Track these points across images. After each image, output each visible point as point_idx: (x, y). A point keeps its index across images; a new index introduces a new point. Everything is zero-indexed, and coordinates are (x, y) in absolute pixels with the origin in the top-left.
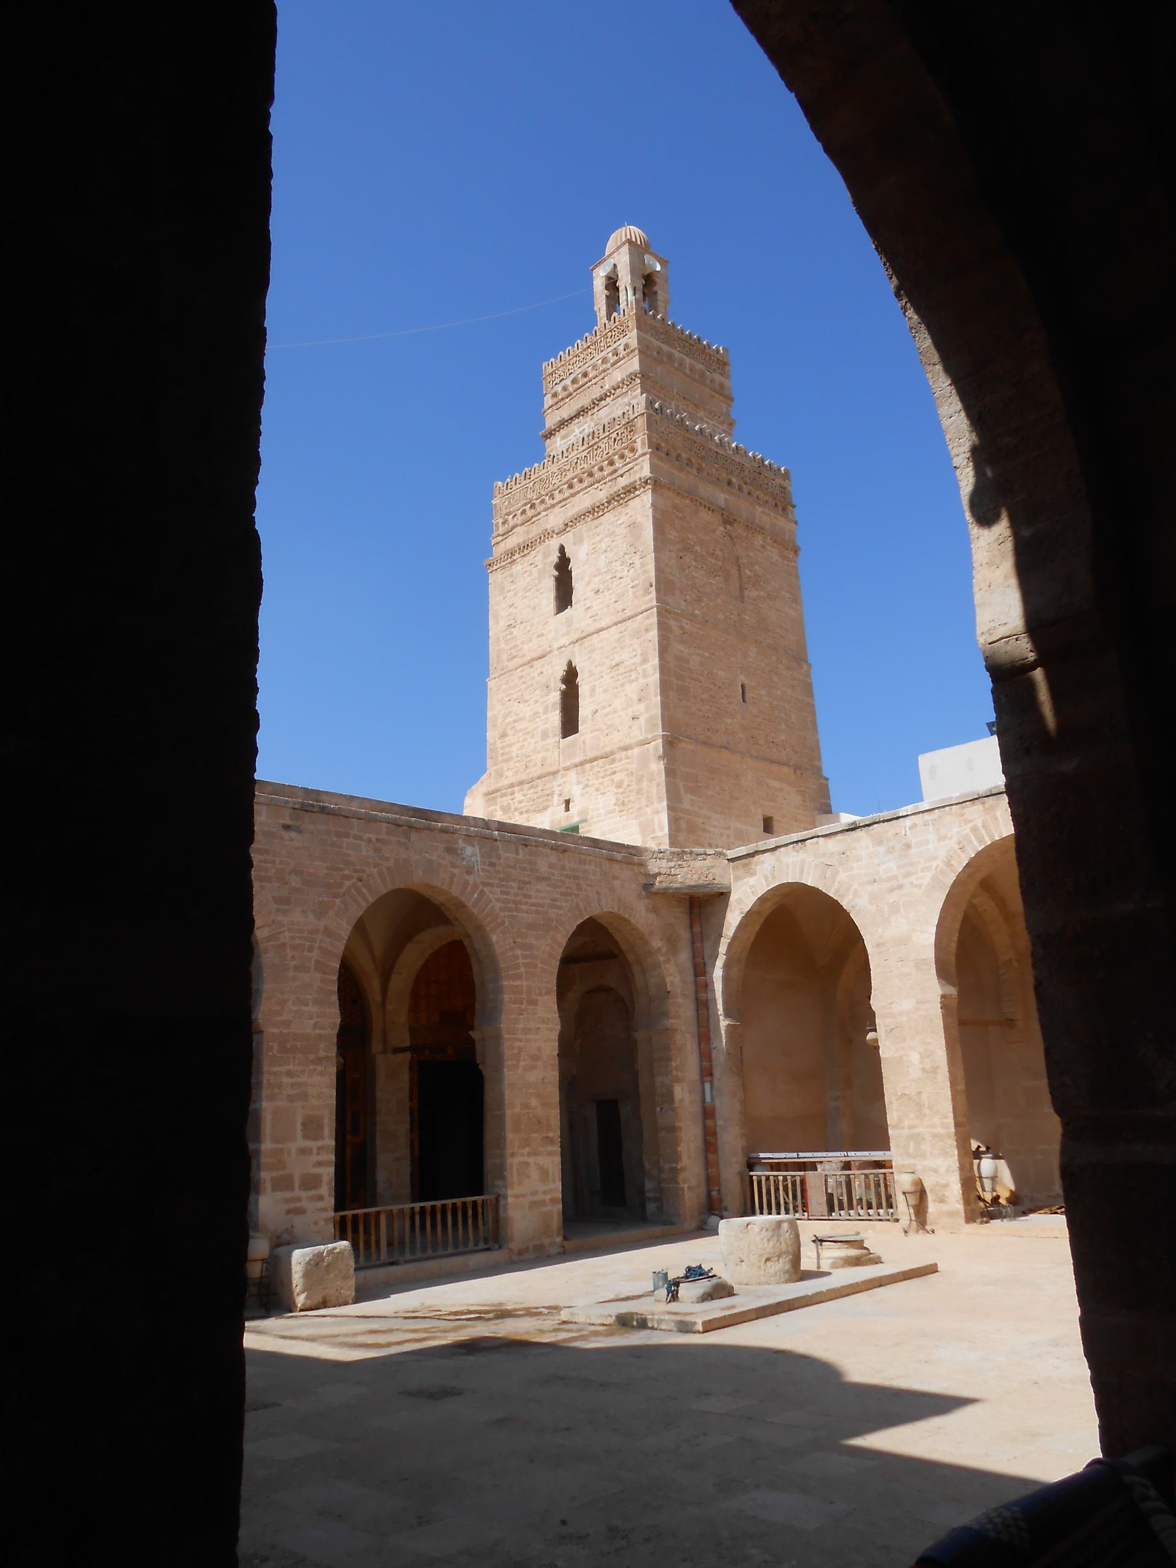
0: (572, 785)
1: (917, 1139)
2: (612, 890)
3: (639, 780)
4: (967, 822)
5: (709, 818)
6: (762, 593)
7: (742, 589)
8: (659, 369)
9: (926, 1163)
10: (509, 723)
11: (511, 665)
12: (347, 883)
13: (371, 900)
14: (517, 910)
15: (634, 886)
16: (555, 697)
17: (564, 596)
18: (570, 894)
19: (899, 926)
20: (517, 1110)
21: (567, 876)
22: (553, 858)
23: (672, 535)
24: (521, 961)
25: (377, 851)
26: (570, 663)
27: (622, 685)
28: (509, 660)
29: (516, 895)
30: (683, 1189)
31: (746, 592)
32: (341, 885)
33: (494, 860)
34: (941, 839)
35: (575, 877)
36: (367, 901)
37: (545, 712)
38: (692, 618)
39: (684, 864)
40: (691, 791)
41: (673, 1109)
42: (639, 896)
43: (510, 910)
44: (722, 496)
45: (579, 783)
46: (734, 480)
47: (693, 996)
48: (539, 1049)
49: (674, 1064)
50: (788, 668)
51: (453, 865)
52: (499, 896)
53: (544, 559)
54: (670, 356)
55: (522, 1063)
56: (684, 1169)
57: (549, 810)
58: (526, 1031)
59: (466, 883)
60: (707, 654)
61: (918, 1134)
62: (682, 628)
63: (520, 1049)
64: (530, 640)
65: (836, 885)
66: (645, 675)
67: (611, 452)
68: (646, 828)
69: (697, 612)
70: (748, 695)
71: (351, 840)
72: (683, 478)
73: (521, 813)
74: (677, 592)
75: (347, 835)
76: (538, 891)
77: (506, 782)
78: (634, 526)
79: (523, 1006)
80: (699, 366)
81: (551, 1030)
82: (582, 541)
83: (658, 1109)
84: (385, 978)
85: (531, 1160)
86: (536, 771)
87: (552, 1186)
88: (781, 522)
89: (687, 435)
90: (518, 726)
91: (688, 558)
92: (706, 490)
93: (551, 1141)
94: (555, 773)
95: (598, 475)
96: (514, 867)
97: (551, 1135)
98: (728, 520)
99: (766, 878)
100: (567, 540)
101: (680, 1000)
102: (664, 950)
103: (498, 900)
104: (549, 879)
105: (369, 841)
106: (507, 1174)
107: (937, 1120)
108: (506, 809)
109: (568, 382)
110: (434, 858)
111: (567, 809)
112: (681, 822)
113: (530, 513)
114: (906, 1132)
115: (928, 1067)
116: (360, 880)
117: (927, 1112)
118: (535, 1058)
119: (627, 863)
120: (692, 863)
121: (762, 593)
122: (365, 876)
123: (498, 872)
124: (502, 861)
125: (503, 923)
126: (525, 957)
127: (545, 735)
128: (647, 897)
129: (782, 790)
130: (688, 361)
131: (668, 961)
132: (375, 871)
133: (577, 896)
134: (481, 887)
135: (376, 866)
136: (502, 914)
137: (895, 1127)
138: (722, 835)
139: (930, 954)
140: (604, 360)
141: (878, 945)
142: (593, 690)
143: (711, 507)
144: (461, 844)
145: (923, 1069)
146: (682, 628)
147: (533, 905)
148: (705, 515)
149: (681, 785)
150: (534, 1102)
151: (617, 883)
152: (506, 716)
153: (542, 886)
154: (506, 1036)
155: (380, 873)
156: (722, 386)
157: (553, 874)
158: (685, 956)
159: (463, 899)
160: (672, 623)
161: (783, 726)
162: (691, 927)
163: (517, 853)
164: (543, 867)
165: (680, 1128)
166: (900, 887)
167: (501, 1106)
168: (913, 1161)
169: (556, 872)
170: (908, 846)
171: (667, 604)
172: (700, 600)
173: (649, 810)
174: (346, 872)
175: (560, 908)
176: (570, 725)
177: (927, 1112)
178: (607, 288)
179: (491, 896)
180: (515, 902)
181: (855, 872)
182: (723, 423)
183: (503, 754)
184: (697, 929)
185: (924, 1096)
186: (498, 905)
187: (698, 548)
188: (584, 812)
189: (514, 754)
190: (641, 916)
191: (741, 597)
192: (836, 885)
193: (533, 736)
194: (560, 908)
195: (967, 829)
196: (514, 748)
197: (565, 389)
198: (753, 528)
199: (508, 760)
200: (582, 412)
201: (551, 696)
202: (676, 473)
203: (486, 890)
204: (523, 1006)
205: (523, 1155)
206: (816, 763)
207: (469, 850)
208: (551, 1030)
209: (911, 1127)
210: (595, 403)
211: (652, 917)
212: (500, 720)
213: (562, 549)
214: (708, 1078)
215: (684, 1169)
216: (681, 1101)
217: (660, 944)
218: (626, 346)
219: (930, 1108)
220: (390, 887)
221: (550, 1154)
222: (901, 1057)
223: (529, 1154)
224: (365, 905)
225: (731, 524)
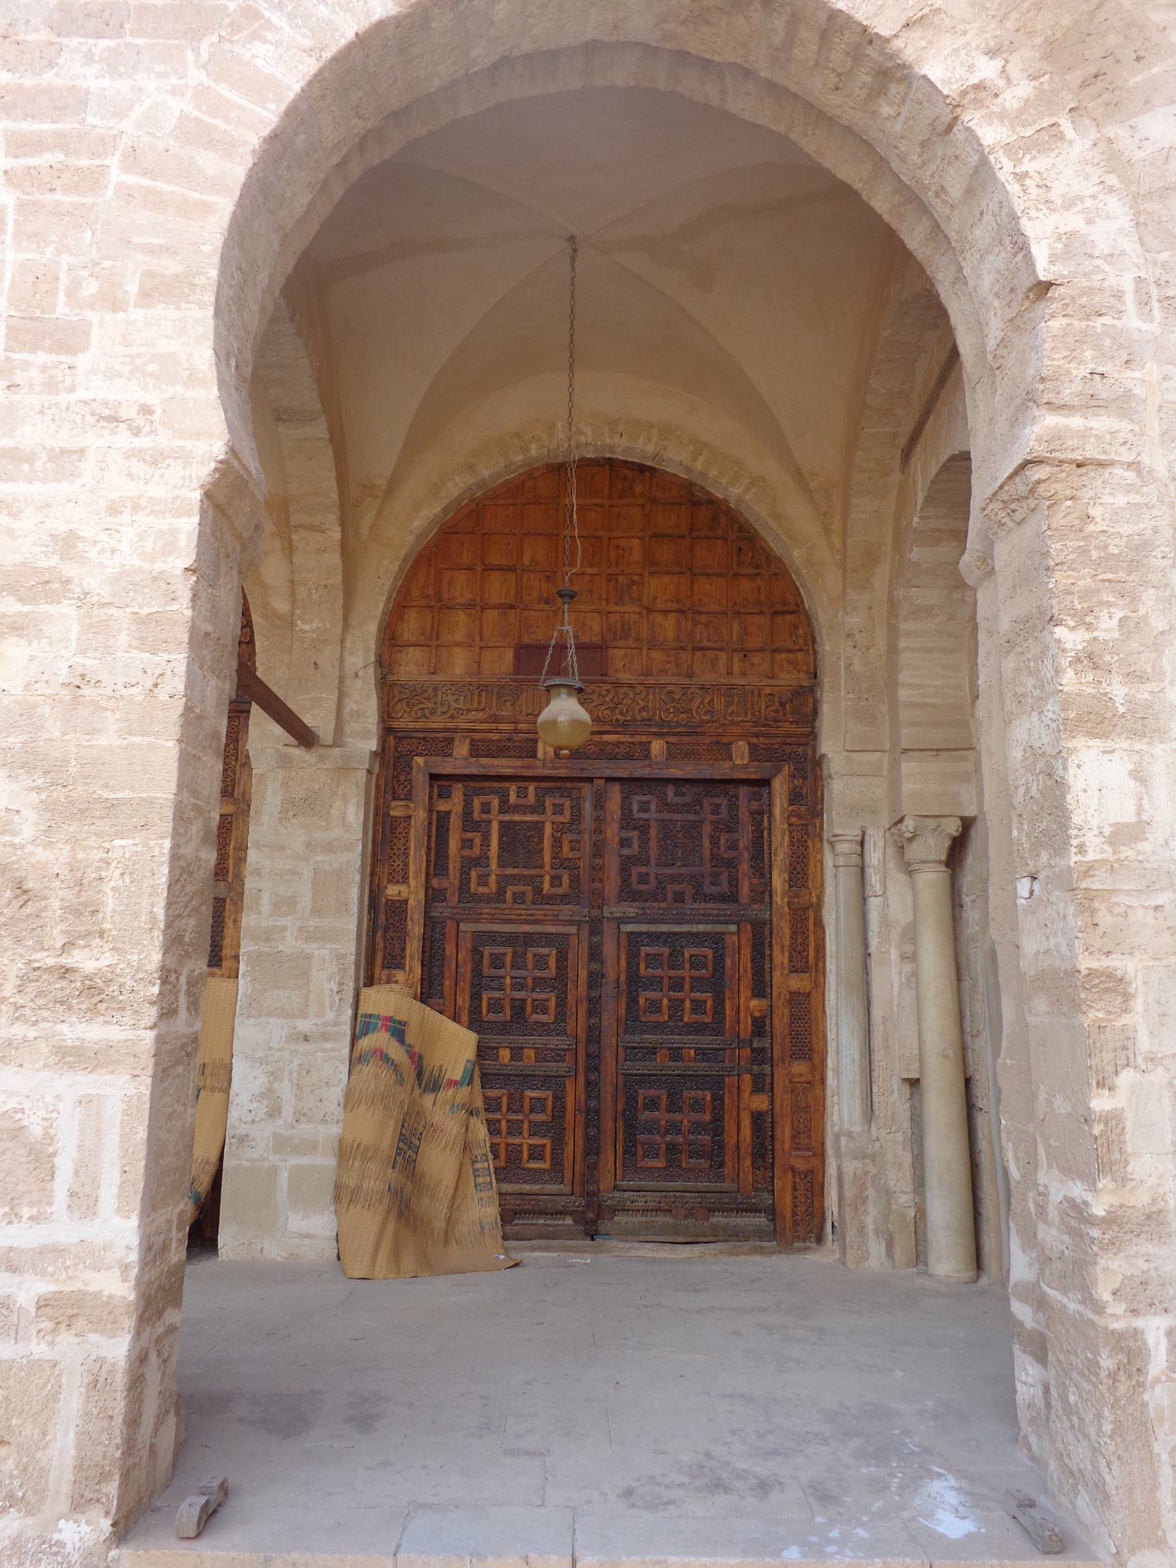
30: (1131, 1350)
41: (1066, 882)
48: (67, 544)
49: (1069, 637)
81: (156, 459)
83: (1023, 887)
87: (63, 1229)
93: (95, 994)
101: (1132, 320)
208: (156, 459)
217: (987, 70)
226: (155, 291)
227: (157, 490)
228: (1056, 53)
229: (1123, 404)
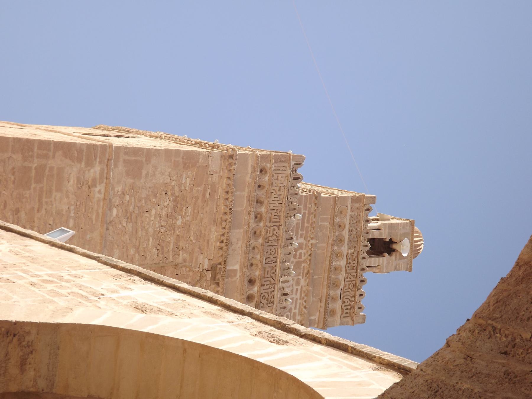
8: (327, 224)
44: (237, 267)
46: (256, 289)
54: (340, 241)
69: (115, 211)
72: (243, 205)
74: (130, 181)
80: (341, 277)
89: (283, 215)
91: (167, 202)
92: (238, 236)
130: (342, 263)
148: (214, 234)
156: (333, 313)
160: (97, 168)
171: (116, 166)
187: (179, 222)
202: (246, 194)
225: (214, 278)
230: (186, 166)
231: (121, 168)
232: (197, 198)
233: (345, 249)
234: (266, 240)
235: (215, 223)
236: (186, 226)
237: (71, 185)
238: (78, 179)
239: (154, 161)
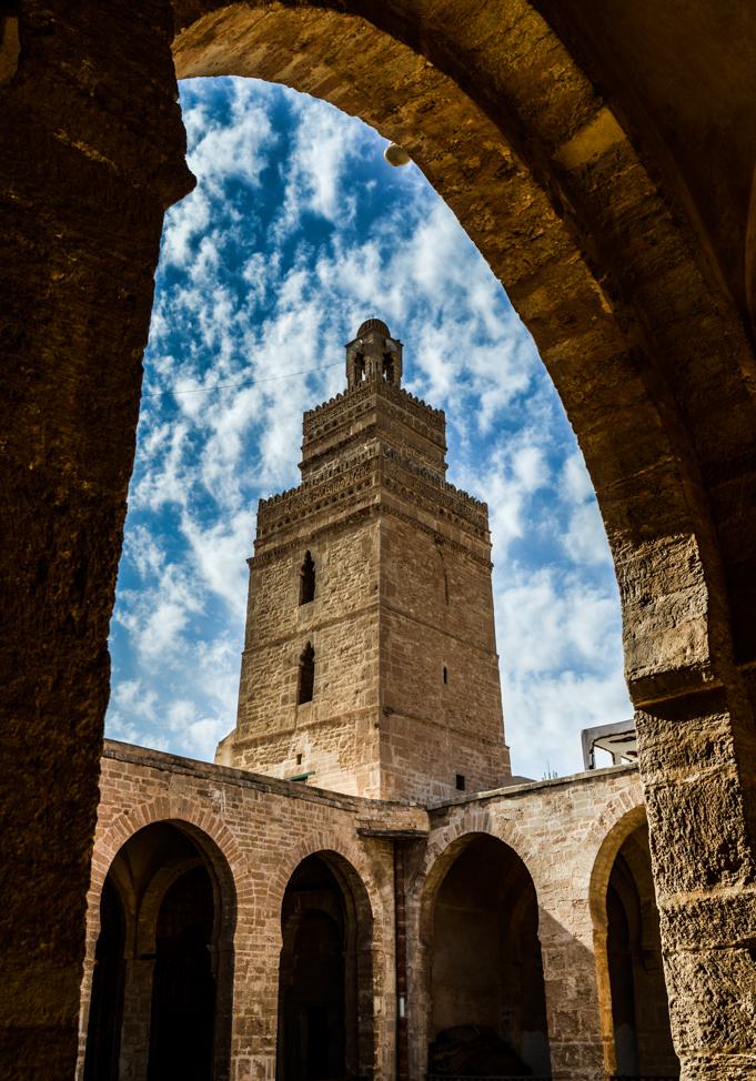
0: (303, 742)
1: (573, 1050)
2: (332, 832)
3: (360, 742)
4: (618, 789)
5: (414, 776)
6: (463, 598)
7: (447, 594)
9: (578, 1071)
10: (257, 689)
11: (262, 643)
12: (116, 816)
13: (134, 831)
14: (253, 845)
15: (350, 829)
16: (295, 670)
17: (308, 594)
18: (297, 834)
19: (561, 872)
20: (242, 1015)
21: (296, 819)
22: (286, 803)
23: (395, 549)
24: (253, 888)
25: (143, 790)
26: (309, 644)
27: (349, 665)
28: (261, 639)
29: (253, 832)
31: (451, 597)
32: (110, 817)
33: (237, 803)
34: (595, 803)
35: (303, 820)
36: (131, 832)
37: (287, 682)
38: (407, 615)
39: (391, 813)
40: (398, 752)
41: (373, 1018)
42: (354, 837)
43: (247, 845)
44: (435, 522)
45: (310, 742)
47: (393, 922)
48: (264, 963)
50: (480, 658)
51: (204, 806)
52: (239, 833)
53: (294, 563)
54: (401, 414)
55: (248, 975)
56: (379, 1070)
57: (284, 762)
58: (254, 947)
59: (213, 821)
60: (418, 644)
61: (573, 1046)
62: (399, 622)
63: (248, 962)
64: (279, 624)
65: (512, 837)
66: (368, 659)
67: (352, 483)
68: (362, 782)
70: (450, 678)
71: (122, 780)
73: (262, 763)
74: (397, 594)
75: (119, 776)
76: (271, 830)
77: (250, 737)
78: (366, 542)
79: (253, 926)
80: (422, 423)
81: (275, 947)
82: (325, 550)
83: (360, 1018)
84: (140, 896)
85: (252, 1058)
86: (274, 730)
88: (479, 544)
90: (264, 692)
91: (406, 568)
92: (423, 517)
93: (269, 1042)
94: (291, 733)
95: (340, 500)
96: (253, 810)
97: (269, 1037)
98: (439, 539)
99: (457, 827)
100: (314, 550)
101: (383, 926)
102: (371, 884)
103: (238, 836)
104: (281, 821)
105: (137, 781)
106: (232, 1073)
107: (588, 1035)
108: (249, 759)
109: (322, 428)
110: (188, 799)
111: (299, 763)
112: (391, 778)
113: (285, 525)
114: (562, 1044)
115: (582, 989)
116: (126, 813)
117: (581, 1027)
118: (260, 970)
119: (346, 810)
120: (398, 813)
121: (463, 598)
122: (131, 811)
123: (240, 813)
124: (243, 804)
125: (241, 855)
126: (257, 885)
127: (285, 700)
128: (360, 839)
129: (472, 755)
130: (414, 418)
131: (374, 893)
132: (139, 806)
133: (303, 836)
134: (225, 825)
135: (141, 802)
136: (241, 848)
137: (555, 1039)
138: (423, 790)
139: (585, 895)
140: (350, 415)
141: (545, 887)
142: (326, 667)
143: (426, 529)
144: (211, 788)
145: (579, 992)
146: (399, 622)
147: (265, 841)
148: (421, 536)
149: (393, 748)
150: (256, 1008)
151: (336, 827)
152: (255, 682)
153: (275, 826)
154: (237, 951)
155: (143, 808)
157: (284, 817)
158: (388, 889)
159: (210, 834)
160: (392, 618)
161: (475, 704)
162: (395, 865)
163: (256, 798)
164: (277, 812)
165: (377, 1034)
166: (564, 840)
167: (229, 1011)
168: (569, 1070)
169: (287, 815)
170: (570, 807)
172: (413, 601)
173: (366, 767)
174: (116, 806)
175: (289, 845)
176: (306, 694)
177: (581, 1027)
178: (356, 361)
179: (233, 833)
180: (252, 839)
181: (529, 826)
182: (438, 467)
183: (249, 714)
184: (400, 867)
185: (579, 1014)
186: (238, 840)
187: (414, 561)
188: (310, 766)
189: (259, 715)
190: (356, 855)
191: (447, 600)
192: (512, 837)
193: (275, 702)
194: (289, 845)
195: (617, 795)
196: (259, 709)
197: (319, 433)
198: (458, 547)
199: (255, 718)
200: (331, 452)
201: (292, 670)
203: (229, 827)
204: (253, 926)
205: (244, 1053)
206: (500, 734)
207: (217, 794)
208: (275, 947)
209: (567, 1040)
210: (343, 445)
211: (363, 855)
212: (249, 687)
213: (308, 554)
214: (403, 993)
215: (379, 1070)
216: (379, 1012)
218: (368, 405)
219: (583, 1025)
220: (151, 821)
221: (268, 1053)
222: (561, 981)
223: (250, 1053)
224: (129, 835)
225: (441, 543)
226: (274, 915)
227: (275, 953)
228: (376, 876)
229: (380, 940)
230: (388, 548)
231: (390, 599)
232: (403, 544)
233: (406, 413)
234: (422, 493)
235: (415, 533)
236: (417, 556)
237: (400, 640)
238: (398, 634)
239: (386, 573)
